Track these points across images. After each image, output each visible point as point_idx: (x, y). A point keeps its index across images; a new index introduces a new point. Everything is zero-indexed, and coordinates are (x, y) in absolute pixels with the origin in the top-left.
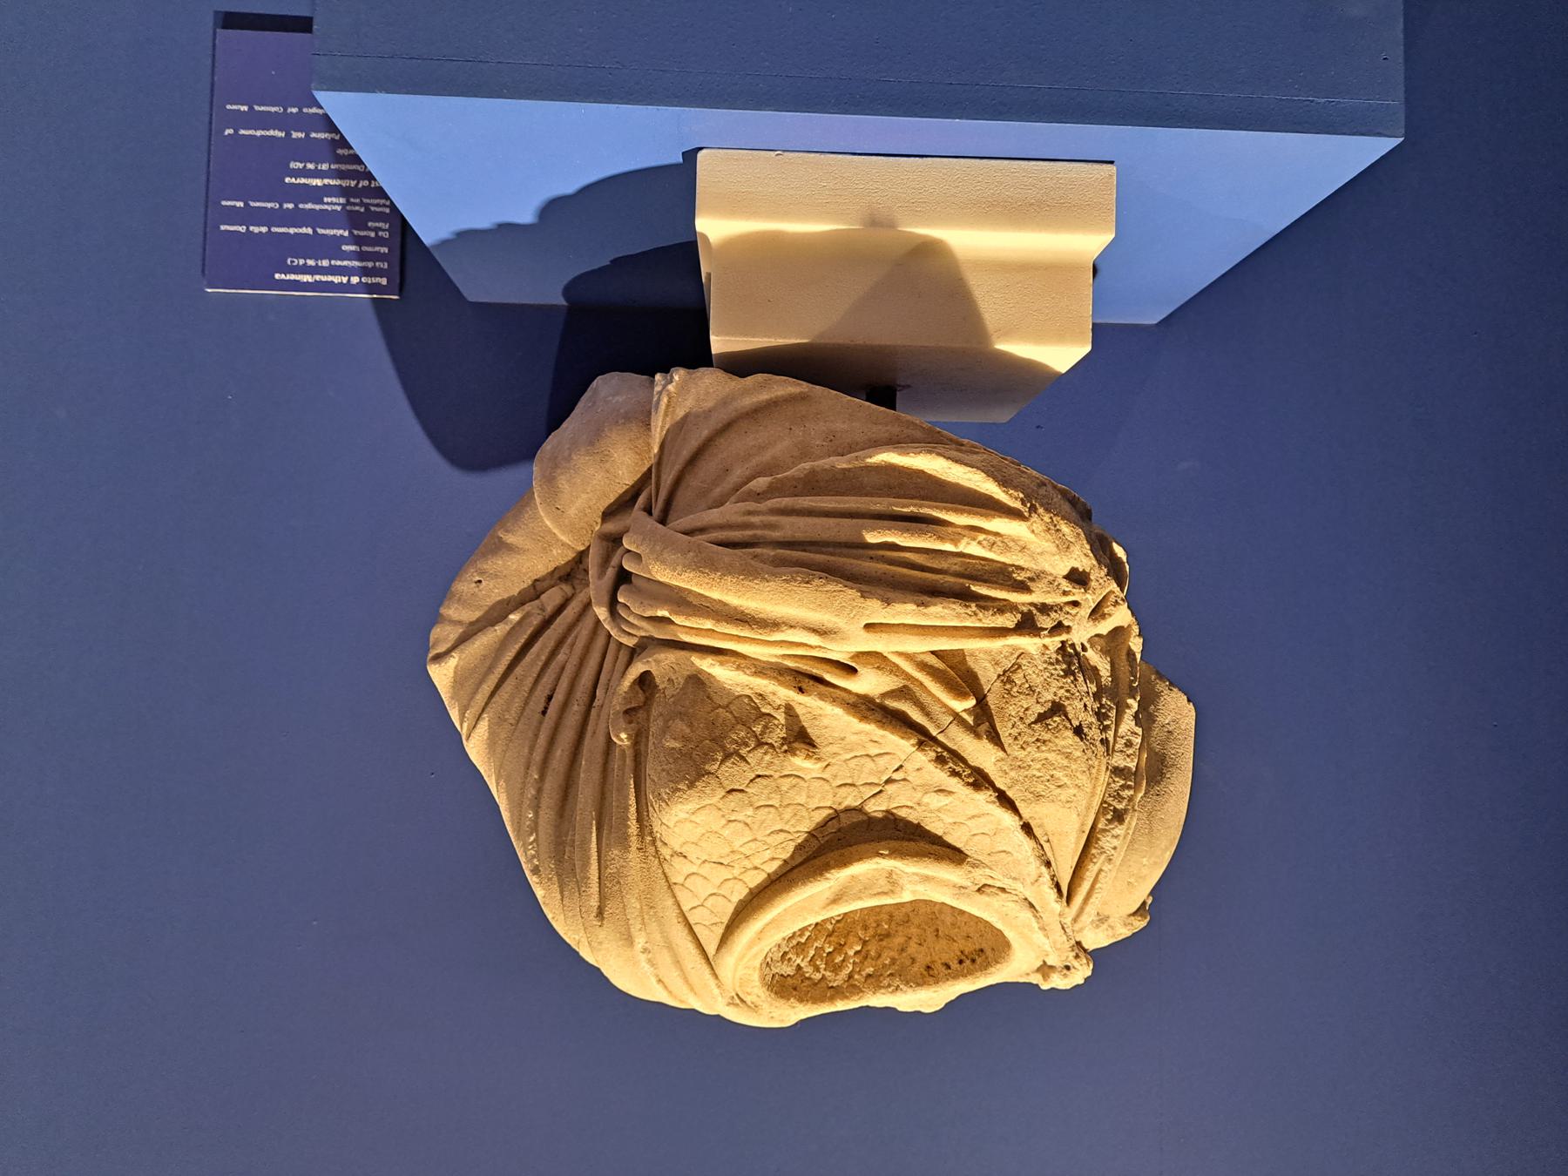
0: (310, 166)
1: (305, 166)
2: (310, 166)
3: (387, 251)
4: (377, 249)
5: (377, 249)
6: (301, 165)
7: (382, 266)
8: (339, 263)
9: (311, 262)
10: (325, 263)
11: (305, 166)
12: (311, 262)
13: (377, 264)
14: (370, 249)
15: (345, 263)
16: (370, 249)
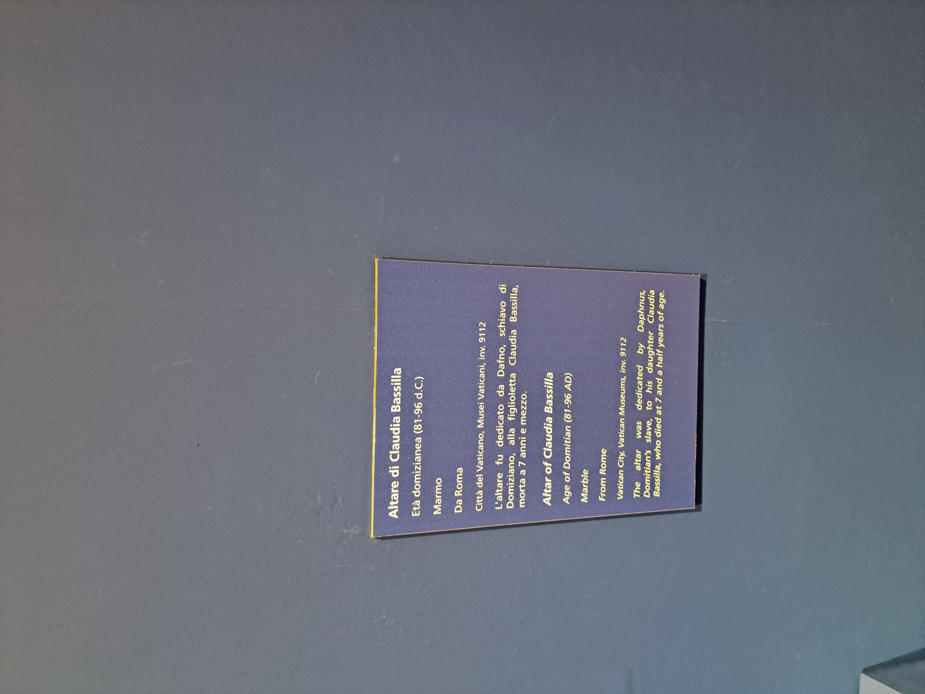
0: (568, 399)
1: (568, 392)
2: (568, 399)
3: (435, 513)
4: (439, 500)
5: (439, 500)
6: (568, 387)
7: (415, 509)
8: (418, 447)
9: (418, 408)
10: (418, 428)
11: (568, 392)
12: (418, 408)
13: (418, 502)
14: (438, 489)
15: (418, 458)
16: (438, 489)
